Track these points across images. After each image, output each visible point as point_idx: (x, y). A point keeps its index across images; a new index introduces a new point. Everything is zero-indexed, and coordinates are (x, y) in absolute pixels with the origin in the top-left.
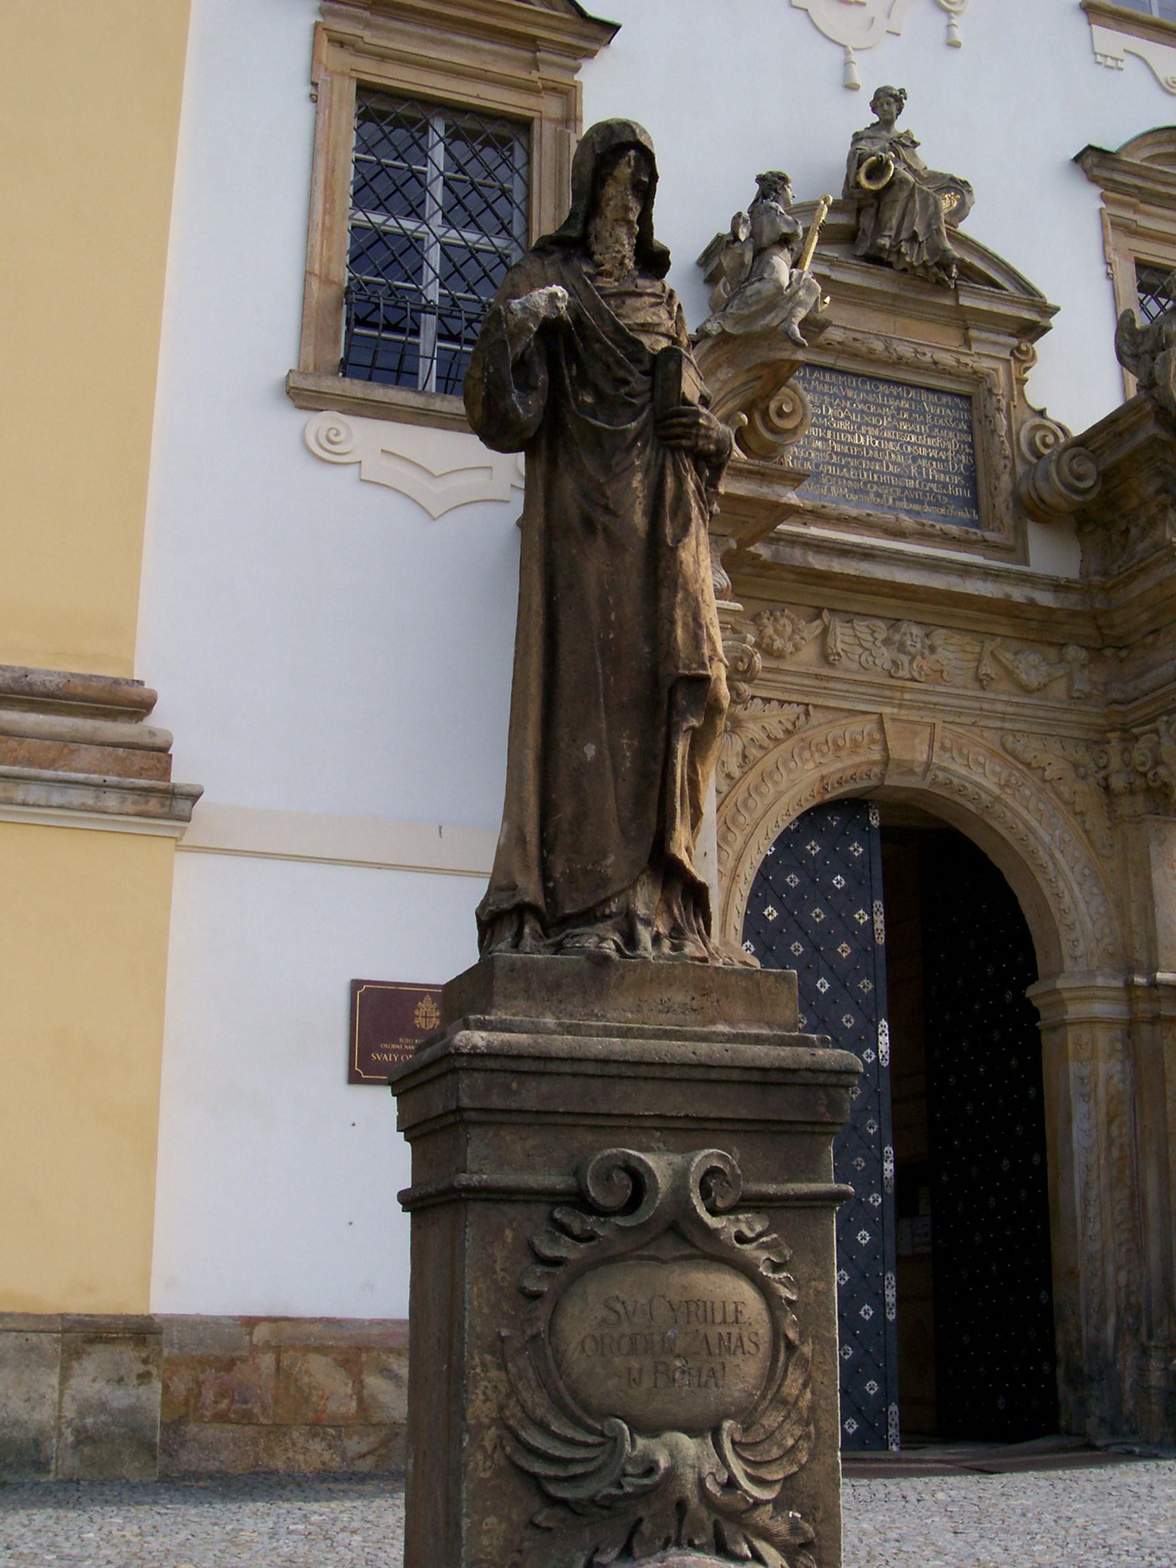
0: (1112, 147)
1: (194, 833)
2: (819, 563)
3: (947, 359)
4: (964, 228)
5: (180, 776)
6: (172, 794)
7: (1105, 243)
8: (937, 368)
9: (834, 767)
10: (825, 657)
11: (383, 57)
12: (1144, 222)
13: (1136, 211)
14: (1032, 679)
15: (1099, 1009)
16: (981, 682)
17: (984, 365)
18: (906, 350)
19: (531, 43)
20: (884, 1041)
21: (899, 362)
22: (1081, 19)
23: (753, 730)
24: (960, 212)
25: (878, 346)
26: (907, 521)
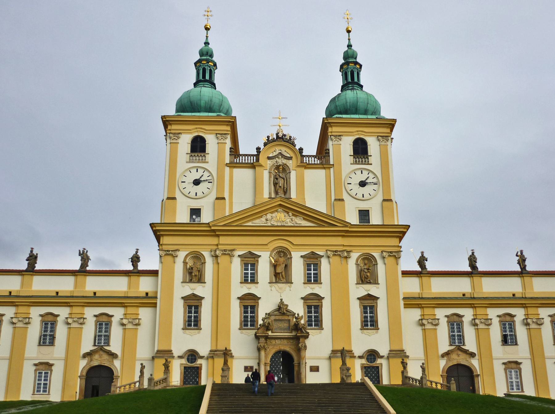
0: (303, 297)
1: (234, 358)
2: (273, 337)
3: (287, 318)
4: (288, 308)
5: (233, 355)
6: (232, 356)
7: (303, 305)
8: (286, 319)
9: (276, 350)
10: (275, 342)
11: (244, 303)
12: (307, 302)
13: (307, 301)
14: (291, 342)
15: (296, 365)
16: (288, 343)
17: (290, 318)
18: (283, 319)
19: (255, 300)
20: (281, 368)
21: (283, 319)
22: (303, 284)
23: (270, 348)
24: (287, 307)
25: (281, 319)
26: (283, 331)
